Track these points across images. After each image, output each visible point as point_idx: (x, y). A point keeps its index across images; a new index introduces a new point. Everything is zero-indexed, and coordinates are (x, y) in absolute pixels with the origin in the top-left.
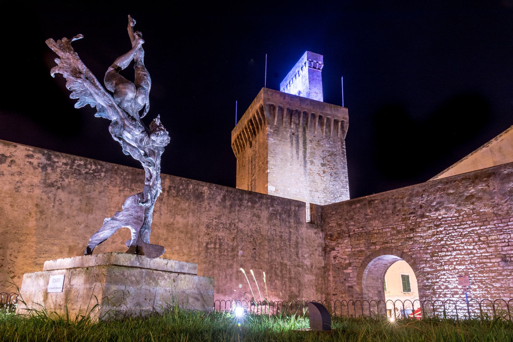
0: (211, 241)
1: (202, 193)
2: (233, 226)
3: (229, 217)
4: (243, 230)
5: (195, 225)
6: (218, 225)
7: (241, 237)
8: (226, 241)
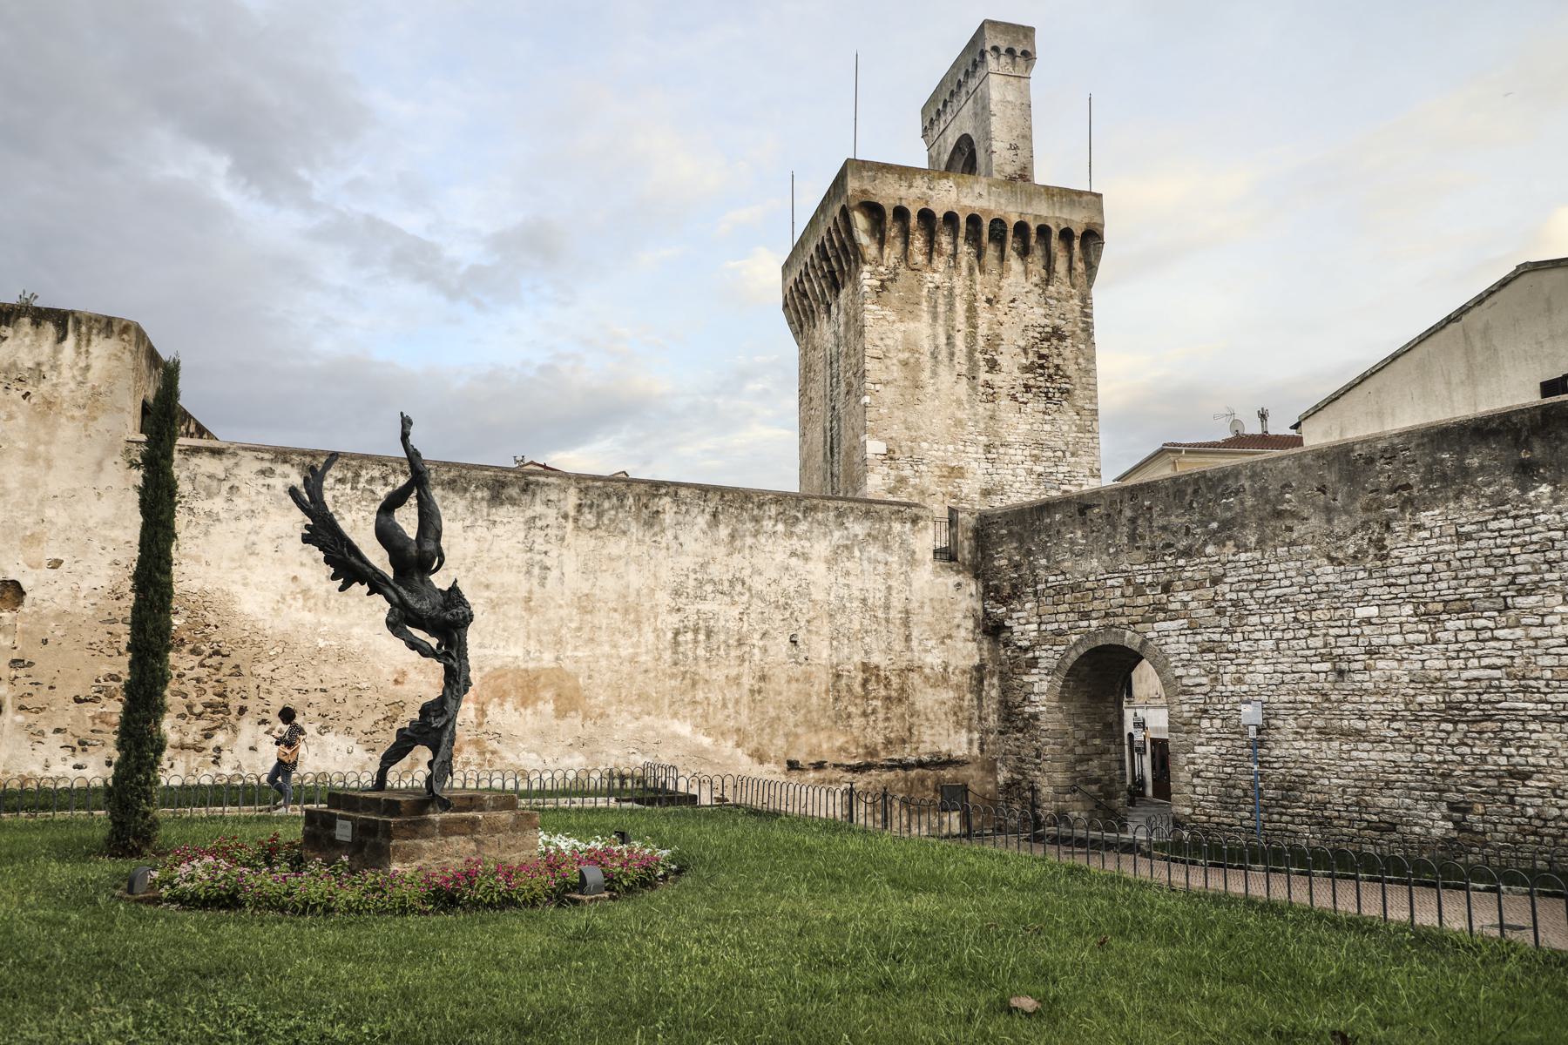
2: (739, 587)
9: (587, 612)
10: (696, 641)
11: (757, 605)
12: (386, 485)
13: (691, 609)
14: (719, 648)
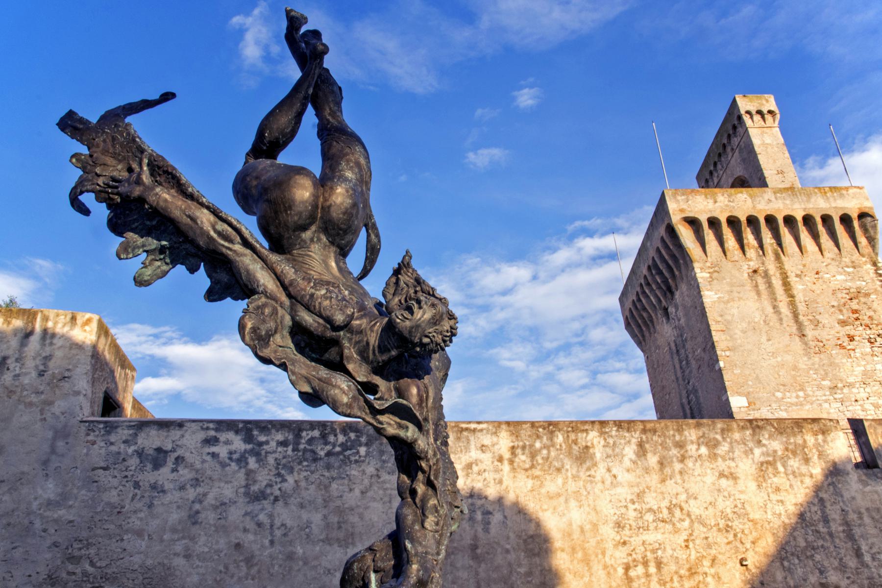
0: (634, 560)
1: (587, 447)
2: (677, 513)
3: (662, 493)
4: (704, 516)
5: (588, 527)
6: (641, 517)
7: (703, 535)
8: (671, 552)
9: (534, 555)
10: (648, 575)
11: (699, 530)
12: (326, 443)
13: (636, 541)
14: (672, 580)
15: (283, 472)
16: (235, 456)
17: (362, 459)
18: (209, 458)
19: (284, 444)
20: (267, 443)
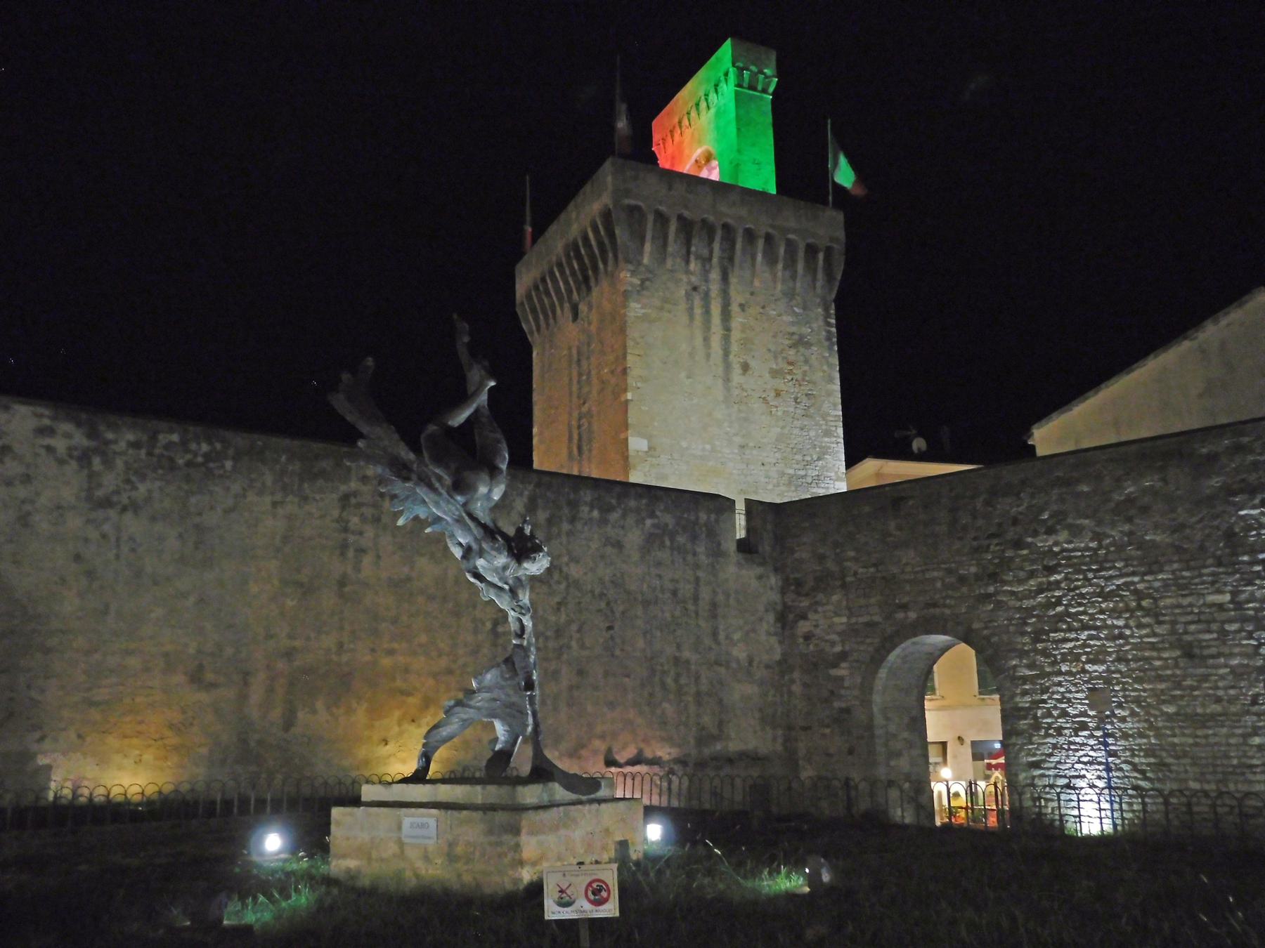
12: (187, 451)
15: (134, 479)
16: (75, 453)
17: (228, 474)
18: (43, 452)
19: (136, 445)
20: (116, 442)
